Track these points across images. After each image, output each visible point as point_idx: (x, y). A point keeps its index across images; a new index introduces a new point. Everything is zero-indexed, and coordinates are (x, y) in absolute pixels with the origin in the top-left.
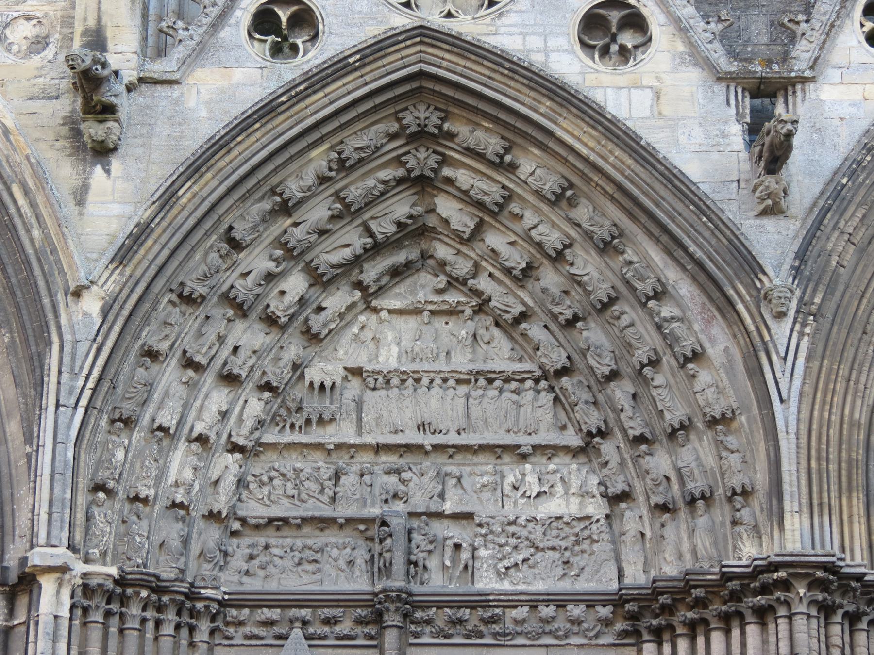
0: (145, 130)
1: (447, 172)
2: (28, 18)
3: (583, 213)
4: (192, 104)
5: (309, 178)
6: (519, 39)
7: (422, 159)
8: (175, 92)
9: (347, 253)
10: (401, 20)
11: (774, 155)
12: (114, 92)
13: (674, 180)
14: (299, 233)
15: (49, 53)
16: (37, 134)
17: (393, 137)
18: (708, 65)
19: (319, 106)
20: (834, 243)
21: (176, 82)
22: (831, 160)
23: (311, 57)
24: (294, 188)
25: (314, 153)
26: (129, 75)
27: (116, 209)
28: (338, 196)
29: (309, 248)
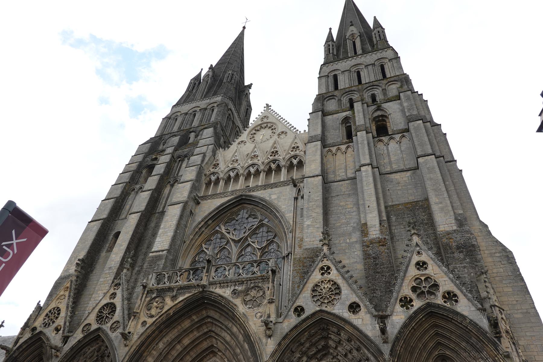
1: (329, 336)
3: (353, 343)
5: (305, 339)
7: (325, 334)
8: (282, 324)
9: (313, 352)
10: (318, 309)
11: (383, 331)
12: (271, 325)
13: (366, 336)
14: (304, 349)
17: (319, 330)
18: (371, 313)
19: (304, 326)
20: (398, 348)
22: (396, 331)
23: (303, 317)
24: (302, 341)
26: (274, 322)
27: (272, 346)
28: (310, 341)
29: (307, 351)
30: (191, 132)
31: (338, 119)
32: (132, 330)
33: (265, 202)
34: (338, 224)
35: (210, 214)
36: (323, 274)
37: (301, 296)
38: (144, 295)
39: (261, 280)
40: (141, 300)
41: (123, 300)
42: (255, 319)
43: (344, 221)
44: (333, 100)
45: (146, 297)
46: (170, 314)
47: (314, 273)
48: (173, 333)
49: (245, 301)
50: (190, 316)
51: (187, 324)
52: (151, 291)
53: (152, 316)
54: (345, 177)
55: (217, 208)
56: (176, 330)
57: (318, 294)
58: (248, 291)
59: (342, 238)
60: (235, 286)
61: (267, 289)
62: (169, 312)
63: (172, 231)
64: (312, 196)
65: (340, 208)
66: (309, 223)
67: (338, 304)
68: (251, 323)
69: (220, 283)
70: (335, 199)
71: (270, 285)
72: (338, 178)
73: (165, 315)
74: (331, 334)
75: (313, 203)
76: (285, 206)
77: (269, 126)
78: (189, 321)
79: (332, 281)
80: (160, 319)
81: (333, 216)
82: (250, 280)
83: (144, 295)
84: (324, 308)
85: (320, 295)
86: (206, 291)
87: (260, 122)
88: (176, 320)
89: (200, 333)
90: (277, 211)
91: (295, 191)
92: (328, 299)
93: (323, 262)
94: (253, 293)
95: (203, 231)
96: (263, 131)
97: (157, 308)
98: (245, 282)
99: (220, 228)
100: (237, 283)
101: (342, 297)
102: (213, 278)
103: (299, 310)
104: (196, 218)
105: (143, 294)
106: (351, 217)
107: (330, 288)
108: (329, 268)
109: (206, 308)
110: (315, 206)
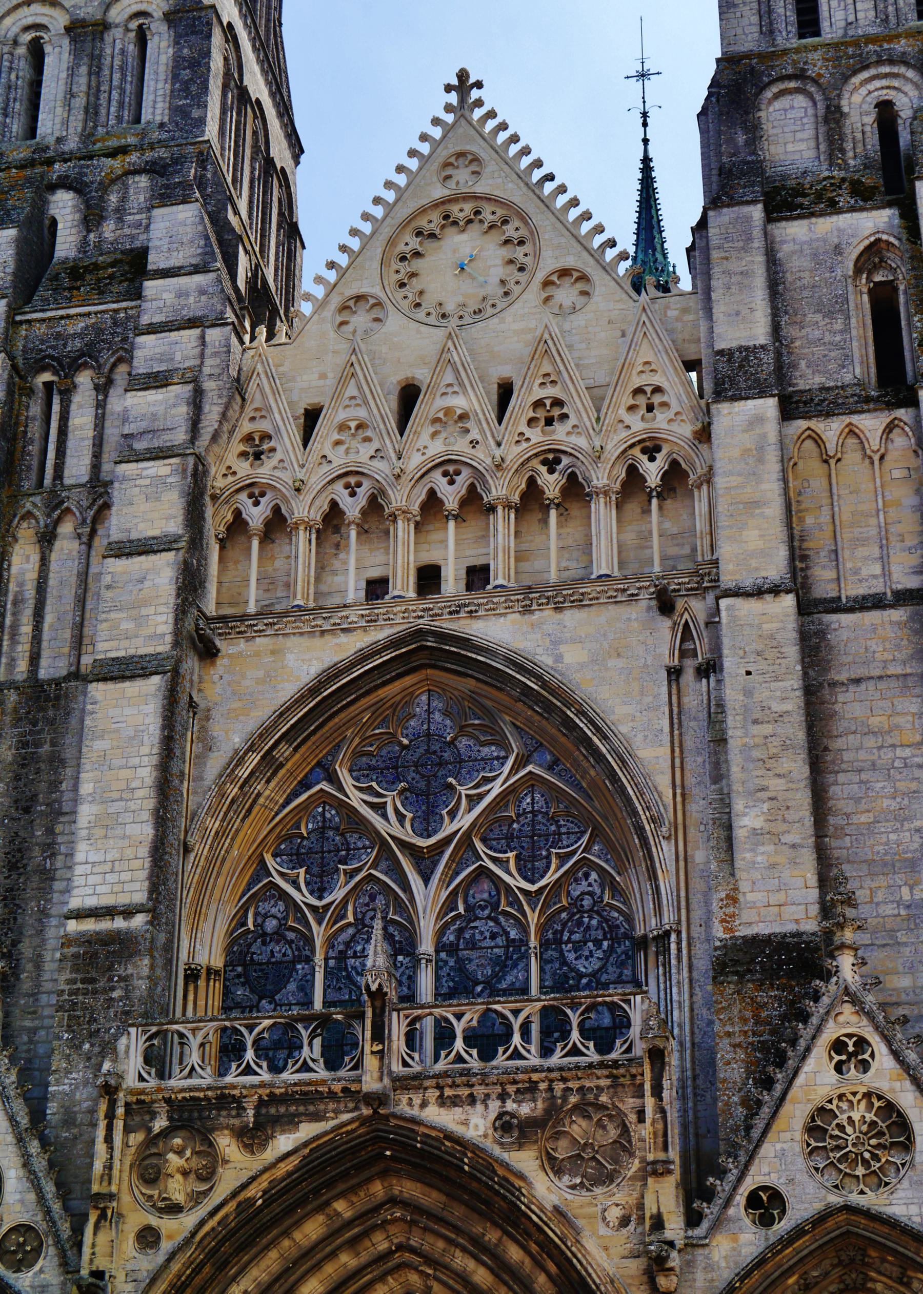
0: (690, 1277)
2: (617, 1205)
4: (716, 1259)
6: (904, 1207)
8: (706, 1251)
10: (834, 1199)
15: (631, 1227)
16: (630, 1281)
17: (834, 1266)
21: (707, 1245)
23: (782, 1227)
25: (791, 1281)
30: (52, 188)
31: (838, 250)
32: (101, 1263)
33: (539, 678)
34: (864, 818)
35: (282, 715)
36: (839, 1068)
37: (768, 1149)
38: (119, 1125)
39: (608, 1082)
40: (109, 1139)
41: (20, 1140)
42: (603, 1230)
43: (886, 802)
44: (800, 101)
45: (127, 1130)
46: (251, 1201)
47: (809, 1066)
48: (264, 1264)
49: (551, 1159)
50: (327, 1203)
51: (312, 1230)
52: (140, 1109)
53: (174, 1209)
54: (877, 587)
55: (313, 691)
56: (273, 1254)
57: (829, 1143)
58: (560, 1122)
59: (881, 881)
60: (503, 1097)
61: (633, 1117)
62: (251, 1192)
63: (146, 816)
64: (762, 694)
65: (870, 742)
66: (758, 823)
67: (905, 1183)
68: (590, 1244)
69: (439, 1087)
70: (849, 696)
71: (649, 1102)
72: (852, 590)
73: (232, 1205)
74: (876, 1281)
75: (767, 729)
76: (626, 710)
77: (487, 216)
78: (321, 1218)
79: (880, 1097)
80: (212, 1223)
81: (841, 778)
82: (564, 1080)
83: (119, 1125)
84: (855, 1199)
85: (838, 1148)
86: (386, 1118)
87: (439, 192)
88: (275, 1222)
89: (364, 1257)
90: (598, 730)
91: (667, 634)
92: (866, 1163)
93: (841, 1019)
94: (578, 1128)
95: (259, 795)
96: (461, 244)
97: (185, 1174)
98: (543, 1086)
99: (333, 779)
100: (511, 1089)
101: (919, 1158)
102: (405, 1064)
103: (766, 1204)
104: (217, 729)
105: (110, 1116)
106: (914, 786)
107: (873, 1124)
108: (862, 1043)
109: (383, 1175)
110: (776, 742)
